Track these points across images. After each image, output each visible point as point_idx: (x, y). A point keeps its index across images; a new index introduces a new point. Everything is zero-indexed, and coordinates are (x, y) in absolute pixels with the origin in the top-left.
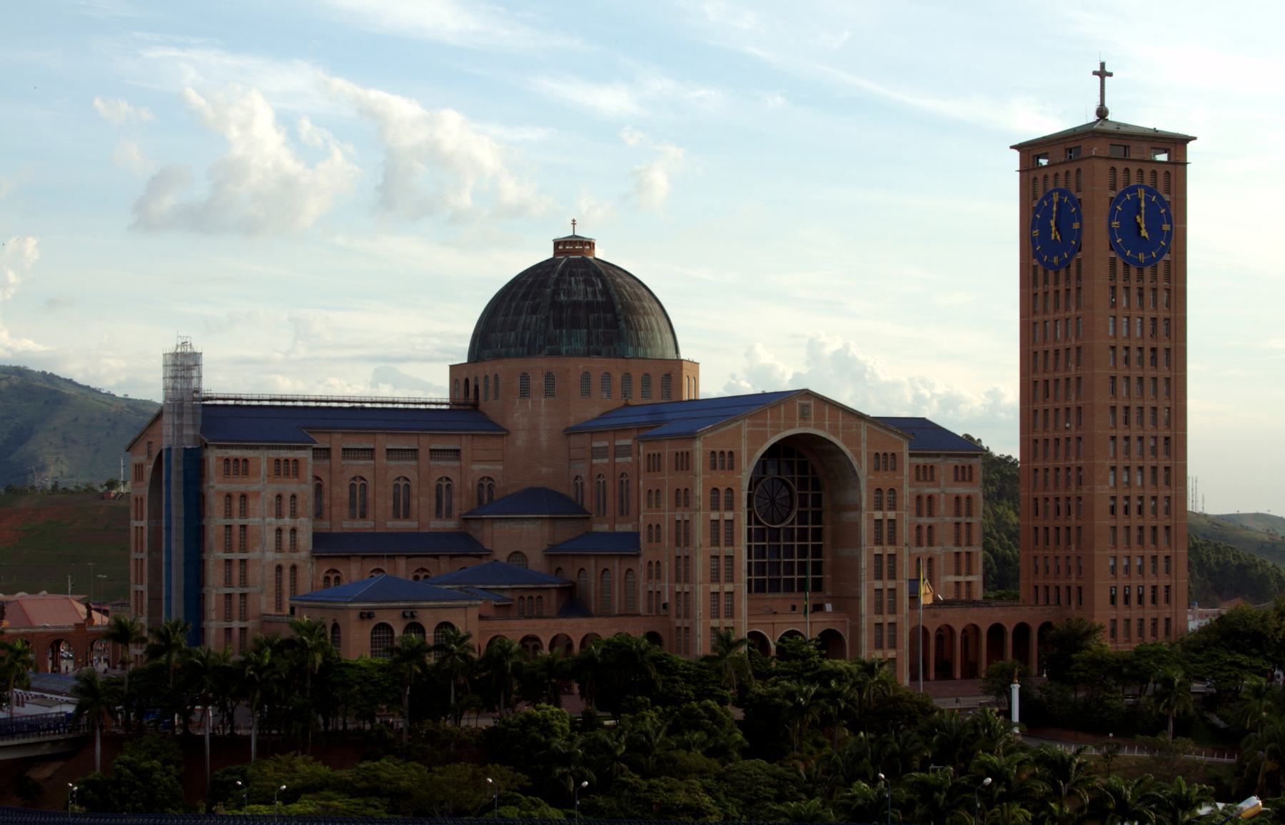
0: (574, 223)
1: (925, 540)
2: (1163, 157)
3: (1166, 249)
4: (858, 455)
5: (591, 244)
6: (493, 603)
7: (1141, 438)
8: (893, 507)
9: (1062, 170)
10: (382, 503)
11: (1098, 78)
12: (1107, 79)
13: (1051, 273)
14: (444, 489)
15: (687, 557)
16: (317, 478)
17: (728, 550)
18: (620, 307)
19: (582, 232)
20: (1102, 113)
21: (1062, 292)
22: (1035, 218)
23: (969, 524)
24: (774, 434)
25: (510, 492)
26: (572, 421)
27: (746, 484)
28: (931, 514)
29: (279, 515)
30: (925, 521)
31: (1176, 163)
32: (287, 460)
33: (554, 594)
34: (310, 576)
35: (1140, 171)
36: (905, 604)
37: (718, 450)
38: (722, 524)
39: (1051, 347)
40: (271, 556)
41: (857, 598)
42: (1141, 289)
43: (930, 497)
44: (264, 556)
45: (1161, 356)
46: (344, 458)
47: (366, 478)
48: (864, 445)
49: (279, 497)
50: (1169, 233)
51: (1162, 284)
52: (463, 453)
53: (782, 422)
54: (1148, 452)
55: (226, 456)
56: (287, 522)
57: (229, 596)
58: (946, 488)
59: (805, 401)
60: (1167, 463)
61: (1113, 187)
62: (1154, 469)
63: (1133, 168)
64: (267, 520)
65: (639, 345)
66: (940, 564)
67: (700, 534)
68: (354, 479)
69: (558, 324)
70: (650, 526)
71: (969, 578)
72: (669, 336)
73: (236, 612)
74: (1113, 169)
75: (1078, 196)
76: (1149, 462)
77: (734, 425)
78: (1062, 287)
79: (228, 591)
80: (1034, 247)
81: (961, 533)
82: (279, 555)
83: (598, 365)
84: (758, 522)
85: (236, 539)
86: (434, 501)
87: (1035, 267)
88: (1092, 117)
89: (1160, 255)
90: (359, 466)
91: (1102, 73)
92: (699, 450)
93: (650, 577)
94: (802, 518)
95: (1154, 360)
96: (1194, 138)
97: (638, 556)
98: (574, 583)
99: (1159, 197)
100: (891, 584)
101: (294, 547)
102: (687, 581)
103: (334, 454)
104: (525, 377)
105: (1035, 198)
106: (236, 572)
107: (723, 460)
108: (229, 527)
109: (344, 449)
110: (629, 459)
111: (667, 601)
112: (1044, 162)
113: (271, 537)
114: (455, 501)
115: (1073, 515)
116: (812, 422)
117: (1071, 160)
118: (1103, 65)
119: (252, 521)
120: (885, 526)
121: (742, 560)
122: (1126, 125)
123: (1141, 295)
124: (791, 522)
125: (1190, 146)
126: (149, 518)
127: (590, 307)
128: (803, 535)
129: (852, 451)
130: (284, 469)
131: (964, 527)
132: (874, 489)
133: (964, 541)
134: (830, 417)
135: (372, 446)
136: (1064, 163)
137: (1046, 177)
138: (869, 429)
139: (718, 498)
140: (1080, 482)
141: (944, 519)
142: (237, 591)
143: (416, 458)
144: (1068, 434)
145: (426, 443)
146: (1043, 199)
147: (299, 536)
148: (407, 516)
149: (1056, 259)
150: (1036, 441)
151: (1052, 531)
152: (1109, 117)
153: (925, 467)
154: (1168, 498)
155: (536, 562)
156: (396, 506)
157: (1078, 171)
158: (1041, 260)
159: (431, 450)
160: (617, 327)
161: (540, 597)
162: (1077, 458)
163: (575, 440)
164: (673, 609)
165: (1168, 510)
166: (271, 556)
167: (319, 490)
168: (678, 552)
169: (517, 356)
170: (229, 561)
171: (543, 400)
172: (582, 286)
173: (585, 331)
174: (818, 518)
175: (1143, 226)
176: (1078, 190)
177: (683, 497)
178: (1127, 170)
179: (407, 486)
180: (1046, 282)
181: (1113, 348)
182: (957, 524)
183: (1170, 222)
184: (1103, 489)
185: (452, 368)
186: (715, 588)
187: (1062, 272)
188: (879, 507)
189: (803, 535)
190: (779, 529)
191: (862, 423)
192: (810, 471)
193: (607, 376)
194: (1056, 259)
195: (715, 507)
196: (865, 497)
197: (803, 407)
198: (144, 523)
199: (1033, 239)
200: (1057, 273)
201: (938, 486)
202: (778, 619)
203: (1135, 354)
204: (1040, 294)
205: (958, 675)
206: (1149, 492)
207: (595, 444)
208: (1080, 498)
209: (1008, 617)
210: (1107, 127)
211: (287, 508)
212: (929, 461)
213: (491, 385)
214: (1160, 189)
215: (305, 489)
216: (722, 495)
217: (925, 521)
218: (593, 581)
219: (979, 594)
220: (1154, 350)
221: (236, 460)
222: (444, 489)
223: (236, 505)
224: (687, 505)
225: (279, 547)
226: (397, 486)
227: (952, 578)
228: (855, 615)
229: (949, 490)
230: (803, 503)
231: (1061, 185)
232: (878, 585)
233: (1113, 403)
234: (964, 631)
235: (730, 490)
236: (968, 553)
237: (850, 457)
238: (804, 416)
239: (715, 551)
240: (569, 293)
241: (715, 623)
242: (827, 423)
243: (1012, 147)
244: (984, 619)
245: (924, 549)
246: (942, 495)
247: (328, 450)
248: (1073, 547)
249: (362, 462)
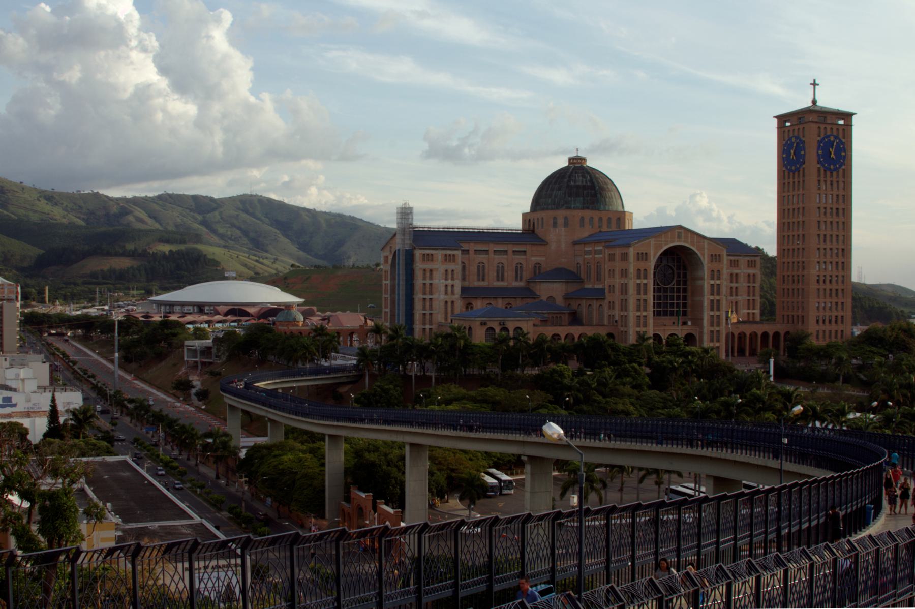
0: (577, 150)
1: (734, 294)
2: (841, 122)
3: (843, 164)
4: (703, 255)
5: (585, 160)
6: (540, 319)
7: (831, 249)
8: (719, 278)
9: (796, 128)
10: (491, 274)
11: (812, 86)
12: (817, 87)
13: (791, 173)
14: (519, 268)
15: (626, 300)
16: (463, 263)
17: (645, 297)
18: (597, 187)
19: (580, 154)
20: (814, 102)
21: (796, 183)
22: (784, 149)
23: (754, 287)
24: (665, 245)
25: (548, 269)
26: (576, 239)
27: (653, 267)
28: (737, 282)
29: (446, 279)
30: (734, 285)
31: (847, 125)
32: (450, 255)
33: (567, 316)
34: (459, 306)
35: (832, 129)
37: (640, 252)
38: (642, 285)
39: (791, 207)
40: (443, 297)
41: (702, 319)
42: (832, 181)
43: (737, 275)
44: (440, 297)
45: (841, 212)
46: (475, 254)
47: (484, 262)
48: (706, 251)
49: (446, 271)
50: (845, 157)
51: (841, 179)
52: (527, 253)
54: (834, 255)
55: (423, 253)
56: (450, 282)
57: (424, 314)
58: (743, 270)
59: (680, 230)
60: (843, 260)
61: (819, 136)
62: (837, 263)
63: (828, 127)
64: (441, 281)
65: (606, 205)
66: (740, 305)
67: (632, 290)
68: (479, 263)
69: (570, 195)
70: (610, 286)
71: (754, 311)
72: (619, 201)
73: (427, 321)
74: (819, 127)
75: (804, 139)
76: (834, 260)
77: (647, 241)
78: (796, 180)
79: (424, 312)
80: (784, 162)
81: (750, 291)
82: (446, 297)
83: (588, 213)
84: (658, 284)
85: (428, 289)
86: (514, 273)
87: (784, 171)
88: (809, 104)
89: (840, 166)
90: (482, 258)
91: (814, 84)
92: (632, 252)
93: (610, 308)
94: (678, 283)
95: (837, 214)
96: (856, 114)
97: (604, 299)
98: (576, 311)
99: (840, 140)
100: (718, 313)
101: (453, 293)
102: (626, 310)
103: (470, 252)
104: (555, 219)
105: (784, 140)
106: (428, 304)
107: (643, 257)
108: (424, 284)
109: (475, 250)
110: (601, 256)
111: (617, 319)
112: (788, 124)
113: (443, 289)
114: (524, 274)
115: (800, 283)
116: (683, 240)
117: (800, 123)
118: (814, 81)
119: (435, 281)
120: (715, 287)
121: (651, 301)
122: (825, 108)
123: (832, 184)
124: (673, 285)
125: (854, 117)
126: (391, 279)
127: (584, 187)
128: (678, 290)
130: (449, 259)
131: (752, 289)
133: (751, 295)
135: (487, 249)
136: (797, 124)
137: (789, 131)
139: (640, 274)
140: (803, 268)
141: (743, 284)
142: (428, 312)
143: (507, 254)
144: (798, 246)
145: (511, 248)
146: (788, 140)
147: (455, 288)
148: (503, 280)
150: (784, 250)
151: (791, 290)
152: (818, 104)
154: (843, 276)
155: (560, 301)
156: (498, 276)
157: (804, 128)
158: (787, 168)
159: (514, 251)
160: (596, 196)
161: (560, 317)
162: (803, 257)
163: (577, 247)
164: (619, 323)
165: (843, 282)
166: (443, 297)
167: (464, 268)
168: (622, 297)
169: (552, 209)
170: (424, 299)
171: (563, 229)
172: (581, 178)
173: (582, 198)
174: (685, 283)
175: (833, 153)
176: (803, 137)
177: (624, 273)
178: (825, 128)
179: (503, 267)
180: (789, 178)
181: (819, 208)
182: (749, 287)
183: (845, 151)
184: (814, 271)
185: (524, 214)
186: (638, 314)
187: (796, 173)
188: (713, 278)
189: (678, 290)
190: (667, 288)
193: (592, 219)
194: (793, 168)
195: (639, 277)
196: (706, 274)
197: (679, 233)
198: (388, 282)
199: (783, 158)
200: (794, 174)
201: (740, 269)
202: (666, 328)
203: (829, 211)
204: (786, 183)
205: (747, 354)
206: (834, 273)
207: (586, 249)
208: (803, 276)
209: (770, 329)
210: (816, 108)
211: (450, 276)
212: (736, 258)
213: (540, 222)
214: (841, 136)
215: (458, 267)
216: (642, 272)
217: (734, 285)
218: (584, 310)
219: (758, 318)
220: (837, 209)
221: (428, 255)
222: (519, 268)
223: (428, 274)
224: (626, 276)
225: (446, 293)
226: (498, 266)
227: (746, 311)
228: (701, 326)
229: (745, 271)
230: (679, 276)
231: (796, 134)
232: (712, 313)
233: (819, 233)
234: (750, 335)
235: (645, 270)
236: (754, 300)
238: (679, 237)
239: (638, 297)
240: (575, 181)
241: (638, 329)
242: (689, 240)
243: (774, 117)
244: (760, 329)
245: (733, 298)
246: (742, 274)
247: (468, 250)
248: (800, 297)
249: (483, 256)
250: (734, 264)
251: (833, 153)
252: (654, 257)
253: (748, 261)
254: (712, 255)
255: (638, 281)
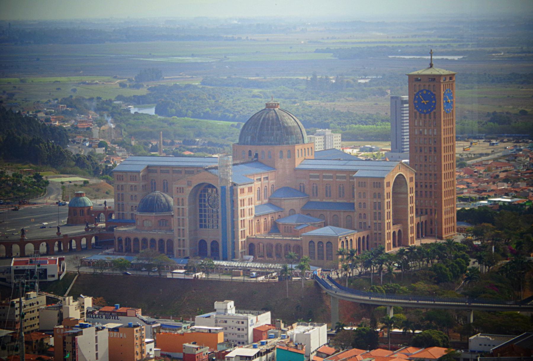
13: (423, 115)
80: (415, 106)
111: (369, 225)
118: (431, 50)
157: (434, 86)
158: (419, 111)
171: (287, 159)
187: (427, 115)
194: (425, 111)
199: (415, 104)
231: (427, 88)
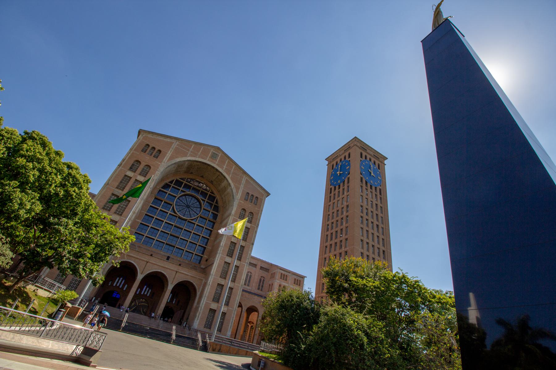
4: (238, 189)
24: (191, 156)
36: (242, 278)
37: (152, 145)
48: (242, 186)
53: (199, 153)
96: (387, 159)
116: (217, 163)
129: (235, 185)
132: (241, 209)
134: (227, 165)
138: (247, 180)
149: (339, 182)
153: (284, 275)
175: (372, 172)
191: (244, 177)
192: (215, 201)
194: (339, 182)
199: (331, 180)
201: (288, 283)
202: (152, 260)
212: (286, 273)
237: (232, 187)
242: (225, 167)
250: (284, 277)
251: (372, 172)
252: (171, 158)
253: (295, 279)
254: (248, 193)
255: (130, 174)
